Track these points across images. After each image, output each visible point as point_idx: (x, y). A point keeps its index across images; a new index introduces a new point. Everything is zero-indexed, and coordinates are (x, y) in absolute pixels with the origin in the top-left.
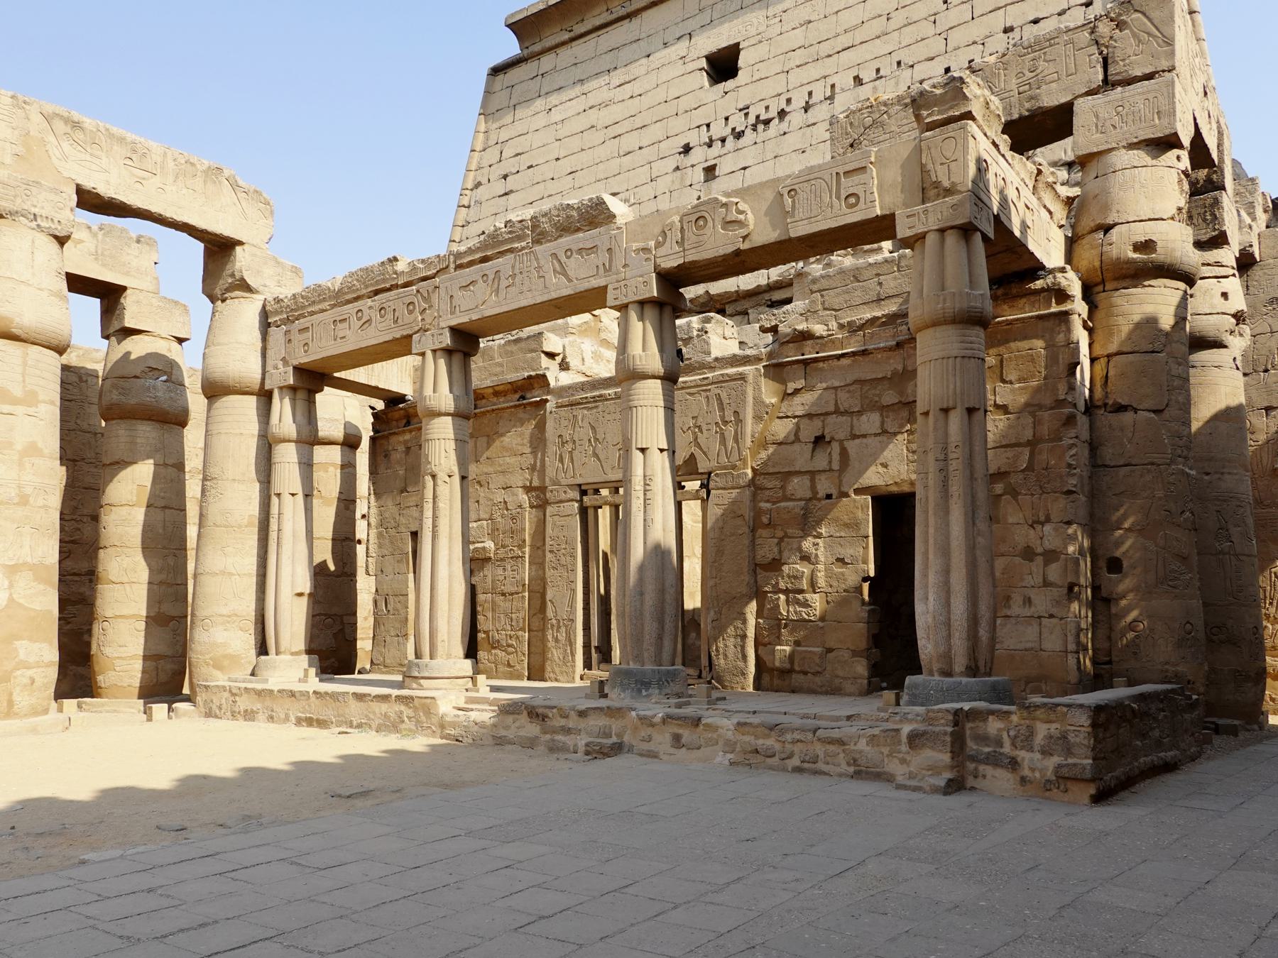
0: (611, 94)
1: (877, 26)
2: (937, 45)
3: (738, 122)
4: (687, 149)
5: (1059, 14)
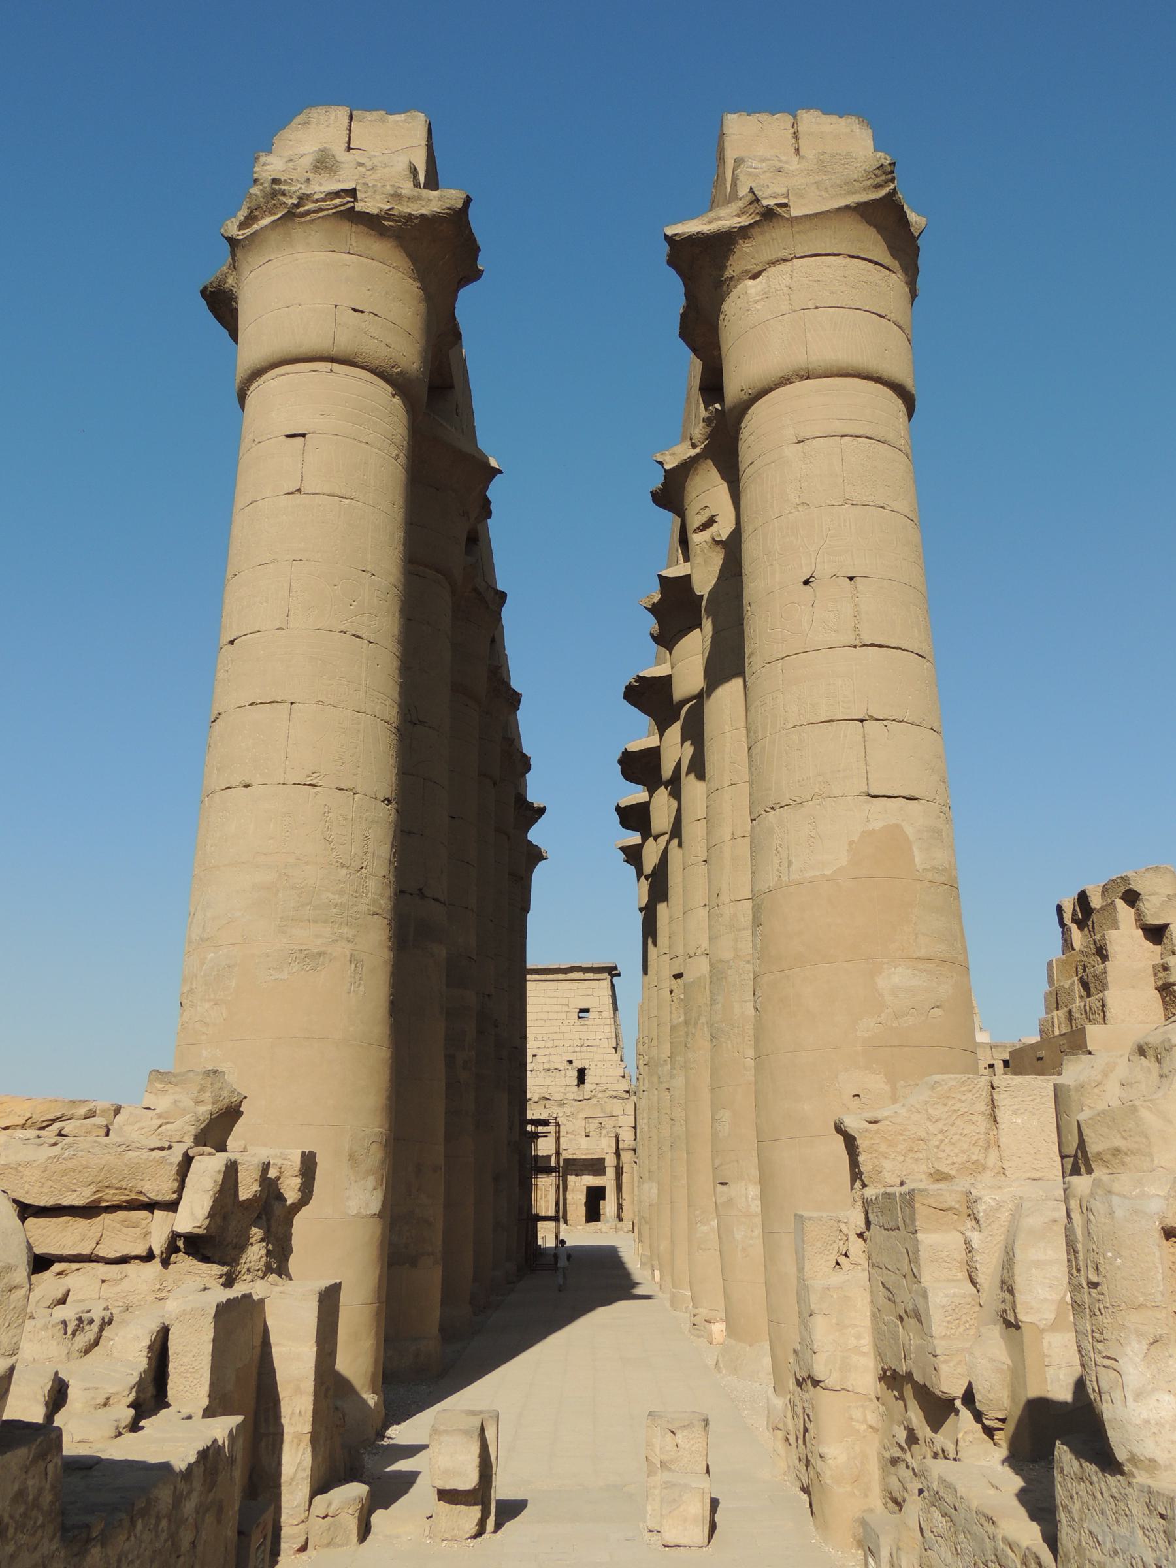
1: (542, 1023)
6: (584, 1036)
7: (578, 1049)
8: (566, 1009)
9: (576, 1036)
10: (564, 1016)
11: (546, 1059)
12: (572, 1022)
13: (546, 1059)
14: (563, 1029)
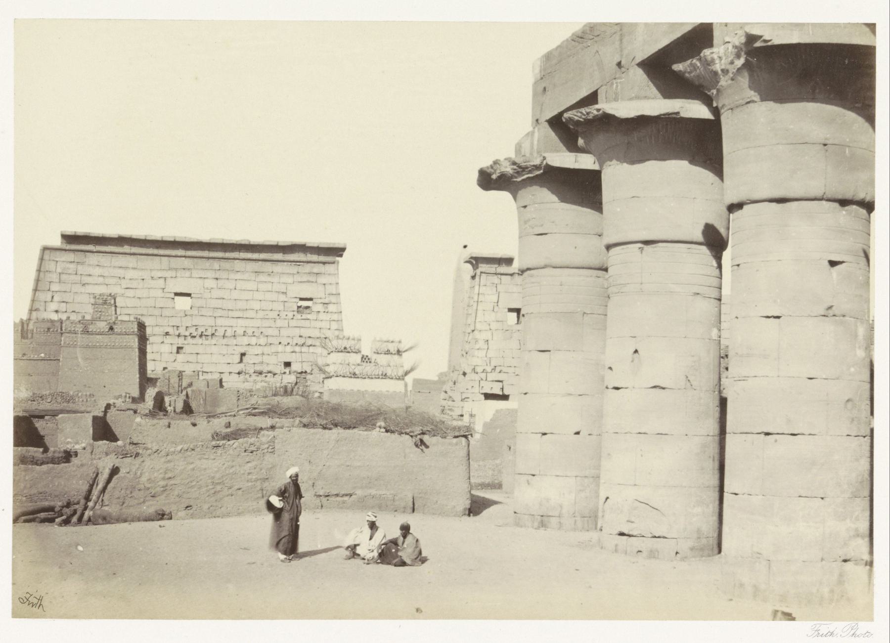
0: (123, 291)
2: (276, 332)
3: (192, 330)
4: (167, 334)
6: (305, 333)
7: (297, 349)
8: (282, 298)
9: (297, 332)
10: (279, 306)
12: (290, 315)
14: (279, 323)
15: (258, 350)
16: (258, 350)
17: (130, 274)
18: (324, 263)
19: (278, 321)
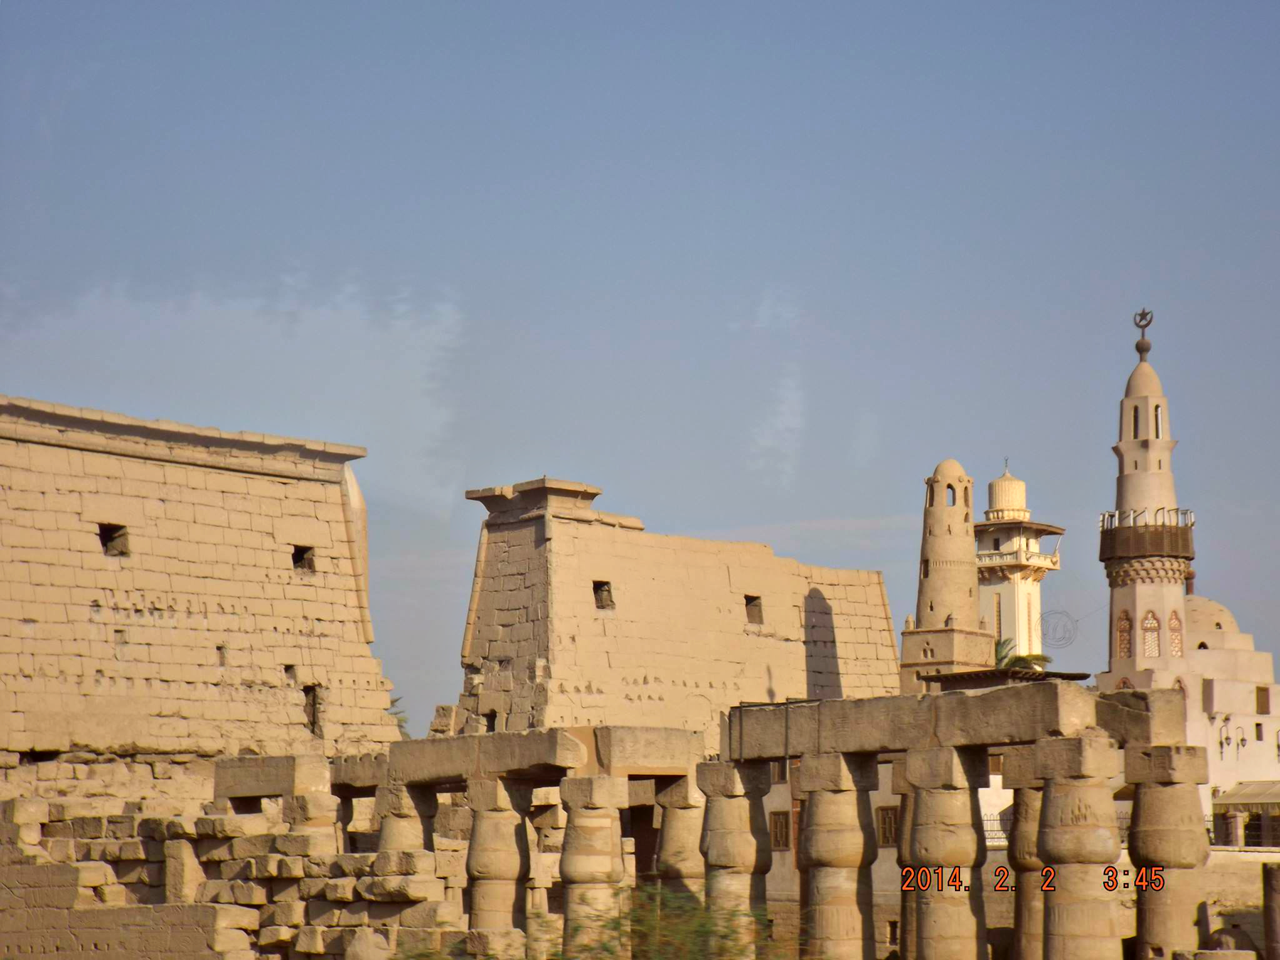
5: (332, 621)
6: (313, 613)
7: (303, 641)
8: (268, 543)
9: (295, 609)
11: (244, 659)
12: (285, 575)
13: (244, 659)
15: (244, 641)
16: (244, 641)
17: (19, 479)
18: (323, 482)
19: (267, 586)
